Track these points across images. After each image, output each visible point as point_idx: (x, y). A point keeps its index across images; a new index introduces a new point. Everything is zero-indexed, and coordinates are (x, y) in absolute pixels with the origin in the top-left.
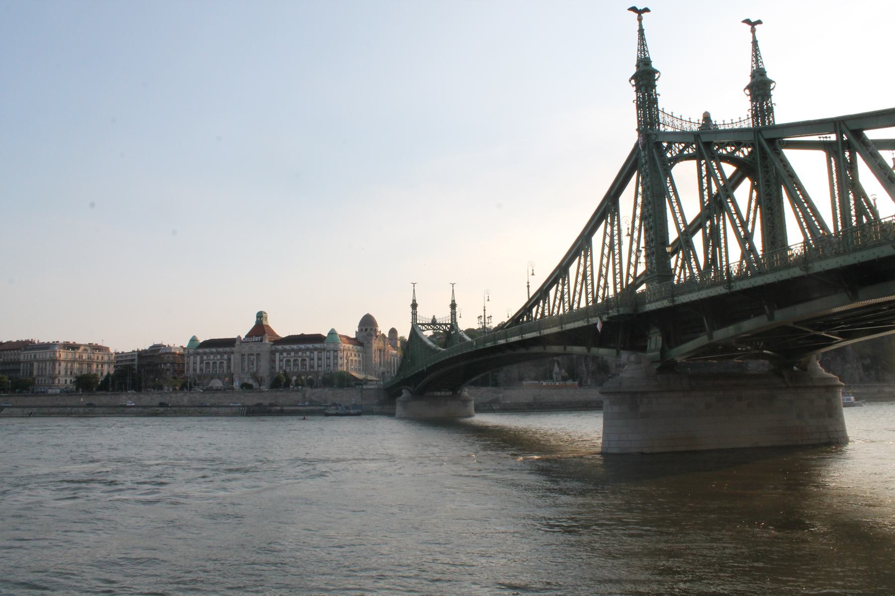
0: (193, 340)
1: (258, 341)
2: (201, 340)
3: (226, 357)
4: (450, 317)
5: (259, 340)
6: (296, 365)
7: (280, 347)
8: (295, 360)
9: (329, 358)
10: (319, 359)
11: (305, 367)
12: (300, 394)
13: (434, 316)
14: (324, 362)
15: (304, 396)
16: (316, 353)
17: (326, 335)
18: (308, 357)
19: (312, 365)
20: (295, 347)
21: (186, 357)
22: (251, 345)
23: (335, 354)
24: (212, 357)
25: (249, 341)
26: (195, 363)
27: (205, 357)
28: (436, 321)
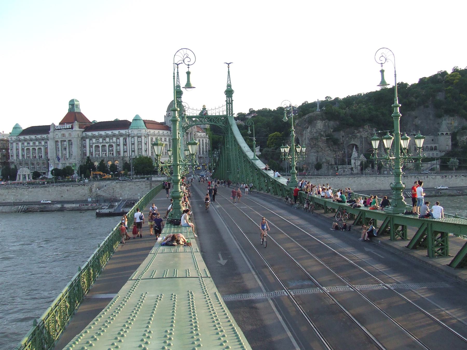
0: (16, 127)
1: (70, 128)
2: (24, 127)
4: (225, 108)
5: (70, 127)
6: (104, 150)
7: (89, 134)
8: (104, 146)
9: (134, 144)
10: (125, 145)
11: (112, 152)
12: (86, 188)
13: (204, 106)
14: (129, 146)
15: (91, 190)
17: (131, 121)
18: (114, 143)
20: (103, 133)
21: (10, 144)
22: (63, 132)
23: (139, 139)
24: (31, 143)
25: (61, 128)
26: (17, 149)
28: (207, 113)
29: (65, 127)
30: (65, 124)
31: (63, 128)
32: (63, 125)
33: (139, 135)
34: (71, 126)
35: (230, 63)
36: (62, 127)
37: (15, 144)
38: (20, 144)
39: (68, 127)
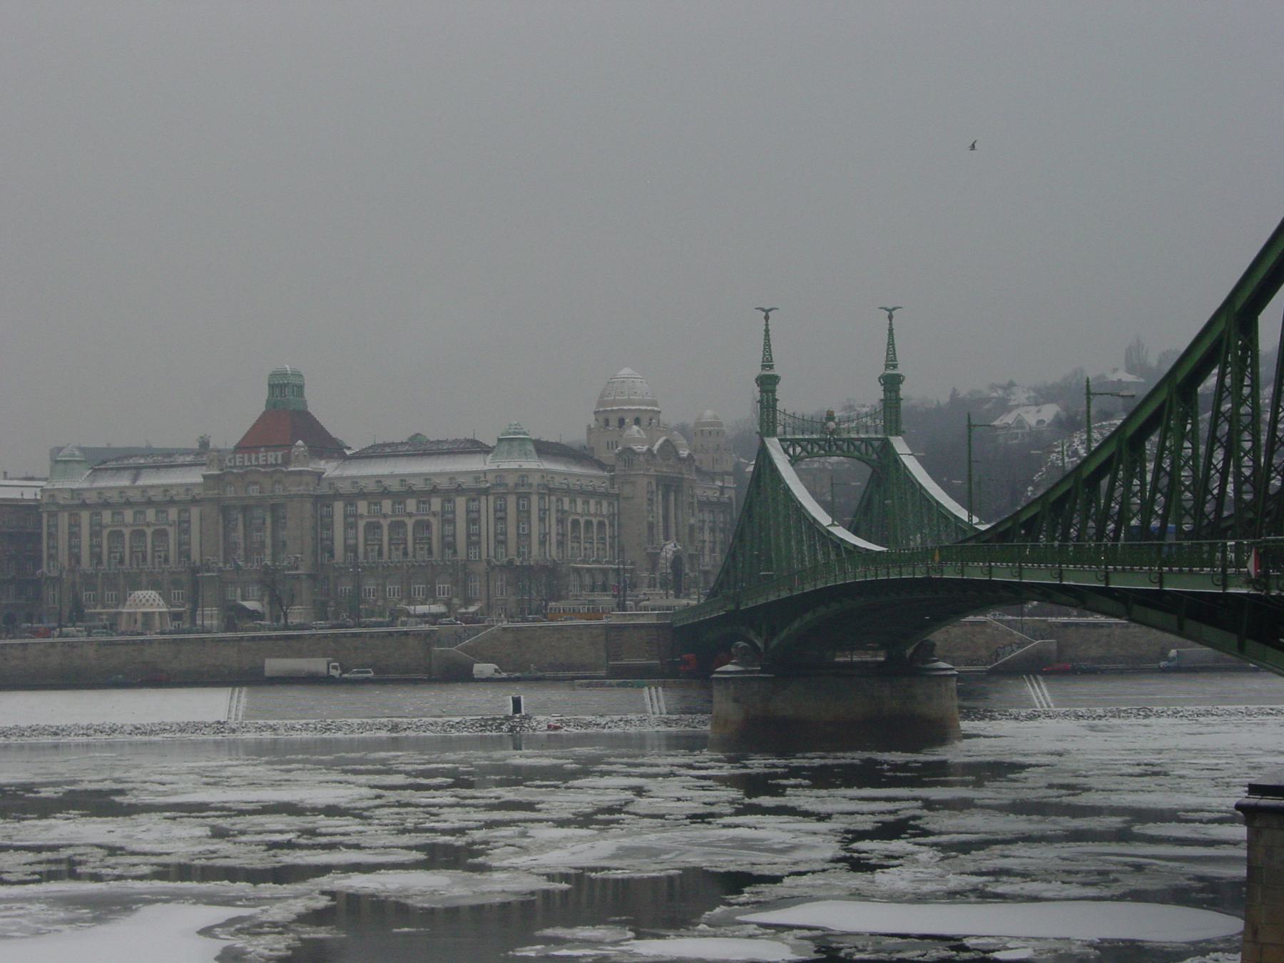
1: (276, 465)
3: (173, 513)
9: (503, 519)
10: (473, 521)
14: (487, 526)
16: (461, 502)
18: (434, 514)
19: (450, 539)
24: (129, 515)
25: (247, 463)
27: (107, 516)
29: (261, 458)
30: (263, 450)
31: (254, 463)
32: (253, 456)
33: (521, 490)
34: (282, 455)
35: (894, 309)
36: (250, 459)
37: (64, 519)
38: (85, 516)
39: (271, 460)
